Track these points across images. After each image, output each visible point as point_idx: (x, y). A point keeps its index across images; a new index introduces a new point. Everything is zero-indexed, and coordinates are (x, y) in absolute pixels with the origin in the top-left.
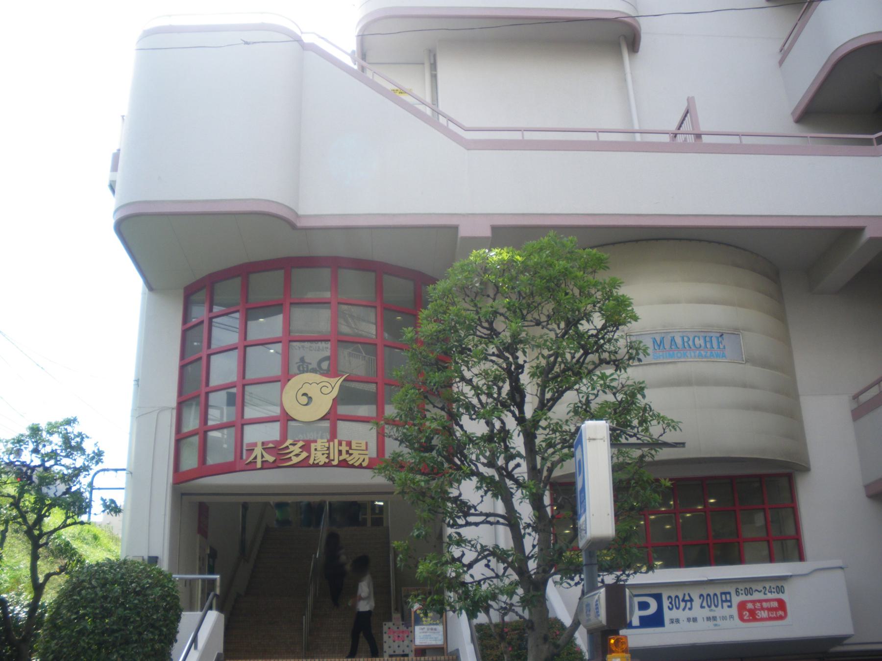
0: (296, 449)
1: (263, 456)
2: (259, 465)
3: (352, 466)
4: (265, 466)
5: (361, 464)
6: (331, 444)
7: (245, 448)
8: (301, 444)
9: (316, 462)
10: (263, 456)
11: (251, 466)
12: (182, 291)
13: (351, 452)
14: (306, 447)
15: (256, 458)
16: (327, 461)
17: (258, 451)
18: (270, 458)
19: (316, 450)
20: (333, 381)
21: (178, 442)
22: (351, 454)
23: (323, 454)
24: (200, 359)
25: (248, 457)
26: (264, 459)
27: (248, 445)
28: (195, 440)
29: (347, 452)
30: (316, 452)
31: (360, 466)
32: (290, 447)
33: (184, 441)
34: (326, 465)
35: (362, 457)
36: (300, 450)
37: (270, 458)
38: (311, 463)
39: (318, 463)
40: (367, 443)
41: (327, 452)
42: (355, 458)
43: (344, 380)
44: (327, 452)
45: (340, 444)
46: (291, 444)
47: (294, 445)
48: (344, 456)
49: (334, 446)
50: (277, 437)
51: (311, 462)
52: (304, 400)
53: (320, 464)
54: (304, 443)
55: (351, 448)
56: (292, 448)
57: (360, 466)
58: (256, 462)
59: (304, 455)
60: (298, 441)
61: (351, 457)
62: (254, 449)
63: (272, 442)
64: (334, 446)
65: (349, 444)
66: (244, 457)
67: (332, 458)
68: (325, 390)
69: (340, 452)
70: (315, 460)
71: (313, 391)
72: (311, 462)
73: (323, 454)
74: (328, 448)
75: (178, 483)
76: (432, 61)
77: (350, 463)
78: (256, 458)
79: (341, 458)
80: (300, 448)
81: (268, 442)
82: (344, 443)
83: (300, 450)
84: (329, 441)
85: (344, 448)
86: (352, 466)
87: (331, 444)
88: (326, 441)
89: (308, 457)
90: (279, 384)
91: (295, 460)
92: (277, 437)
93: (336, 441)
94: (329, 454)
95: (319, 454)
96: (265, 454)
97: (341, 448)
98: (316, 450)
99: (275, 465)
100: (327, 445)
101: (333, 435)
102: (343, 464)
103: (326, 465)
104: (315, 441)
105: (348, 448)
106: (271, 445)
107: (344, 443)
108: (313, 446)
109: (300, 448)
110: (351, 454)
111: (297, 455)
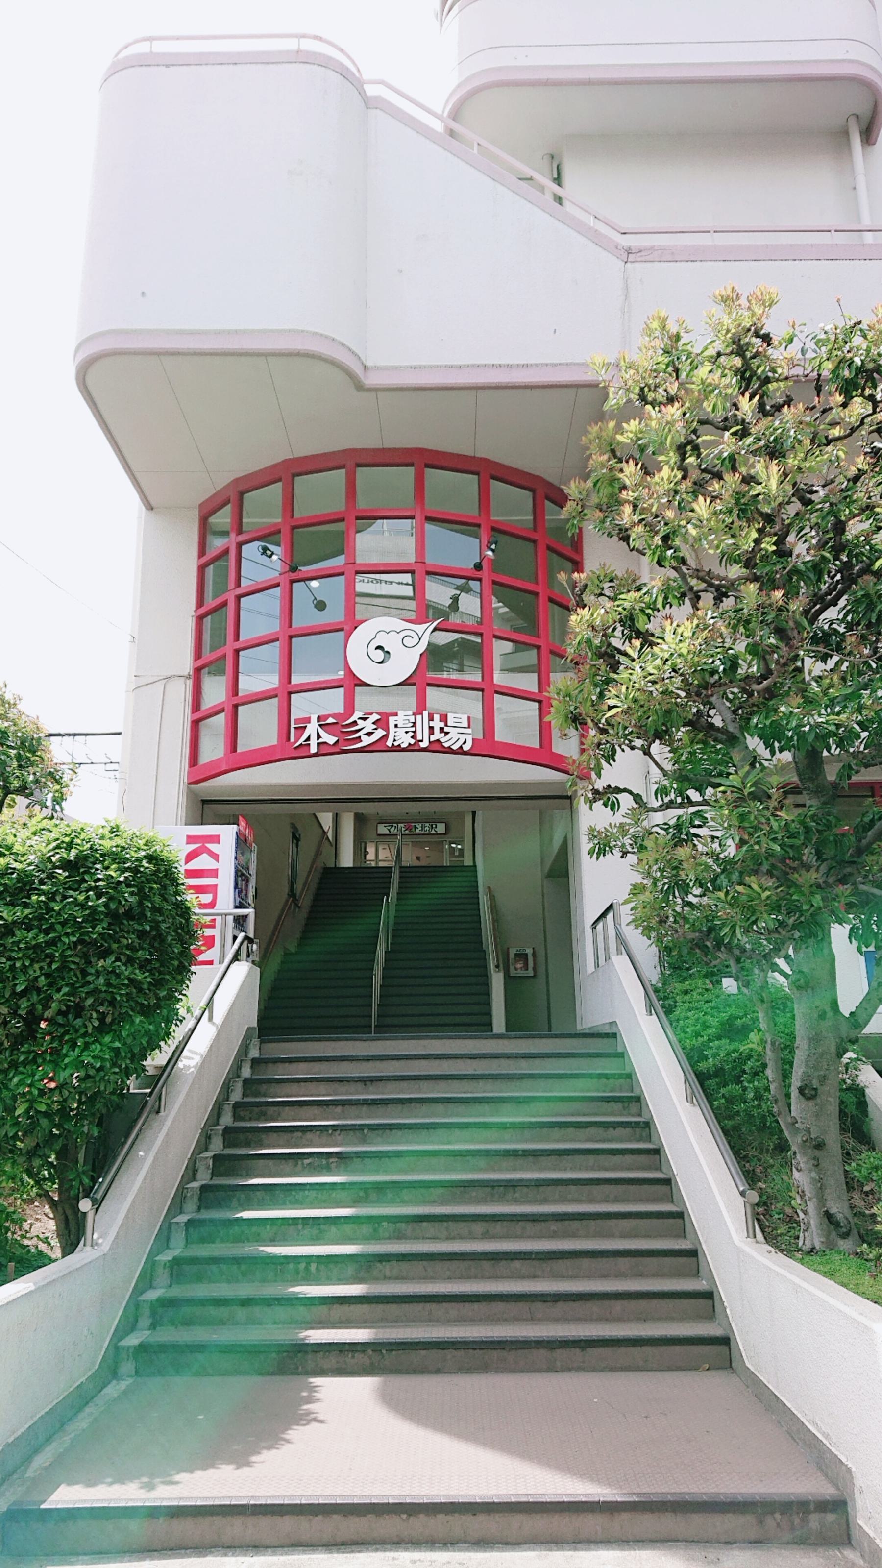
0: (368, 726)
1: (319, 737)
2: (314, 749)
3: (449, 751)
4: (324, 750)
5: (461, 747)
6: (419, 717)
7: (293, 725)
8: (376, 717)
9: (396, 744)
10: (319, 737)
11: (302, 752)
12: (196, 512)
13: (446, 729)
14: (382, 722)
15: (308, 739)
16: (412, 741)
17: (312, 729)
18: (331, 740)
19: (396, 726)
20: (420, 628)
21: (195, 724)
22: (447, 733)
23: (407, 732)
24: (225, 604)
25: (297, 739)
26: (321, 740)
27: (297, 721)
28: (220, 720)
29: (442, 729)
30: (396, 729)
31: (460, 751)
32: (359, 722)
33: (201, 724)
34: (410, 749)
35: (462, 738)
36: (375, 727)
37: (331, 740)
38: (390, 745)
39: (399, 745)
40: (469, 718)
41: (413, 729)
42: (453, 740)
43: (435, 630)
44: (413, 729)
45: (431, 718)
46: (360, 718)
47: (365, 719)
48: (437, 735)
49: (423, 721)
50: (339, 708)
51: (389, 743)
52: (379, 655)
53: (403, 746)
54: (379, 717)
55: (446, 725)
56: (361, 723)
57: (460, 751)
58: (309, 745)
59: (380, 733)
60: (371, 714)
61: (448, 736)
62: (305, 727)
63: (334, 716)
64: (423, 721)
65: (444, 718)
66: (292, 739)
67: (419, 737)
68: (408, 642)
69: (431, 729)
70: (395, 740)
71: (391, 643)
72: (389, 743)
73: (407, 732)
74: (414, 724)
75: (196, 783)
76: (555, 176)
77: (446, 745)
78: (308, 739)
79: (433, 738)
80: (373, 723)
81: (327, 717)
82: (437, 717)
83: (375, 727)
84: (415, 714)
85: (437, 724)
86: (449, 751)
87: (419, 717)
88: (411, 713)
89: (386, 737)
90: (342, 634)
91: (366, 741)
92: (339, 708)
93: (425, 713)
94: (415, 732)
95: (401, 732)
96: (322, 732)
97: (432, 724)
98: (396, 726)
99: (337, 750)
100: (412, 719)
101: (421, 706)
102: (437, 748)
103: (410, 749)
104: (396, 714)
105: (442, 725)
106: (331, 720)
107: (437, 717)
108: (392, 721)
109: (373, 723)
110: (447, 733)
111: (369, 734)
